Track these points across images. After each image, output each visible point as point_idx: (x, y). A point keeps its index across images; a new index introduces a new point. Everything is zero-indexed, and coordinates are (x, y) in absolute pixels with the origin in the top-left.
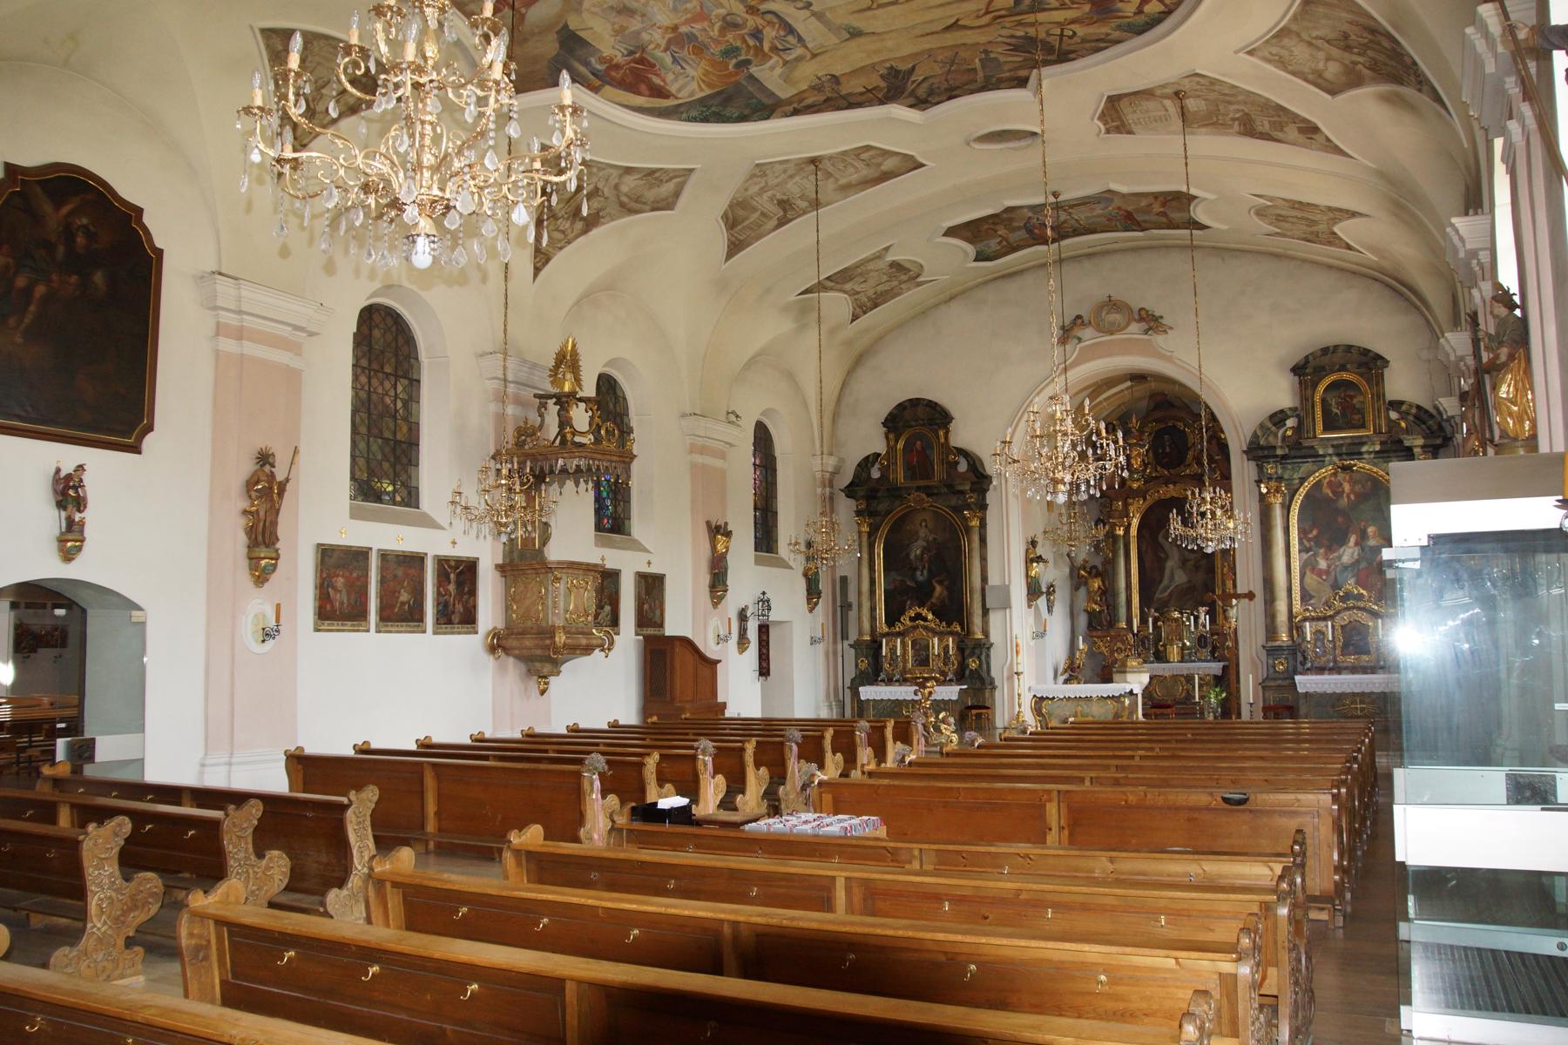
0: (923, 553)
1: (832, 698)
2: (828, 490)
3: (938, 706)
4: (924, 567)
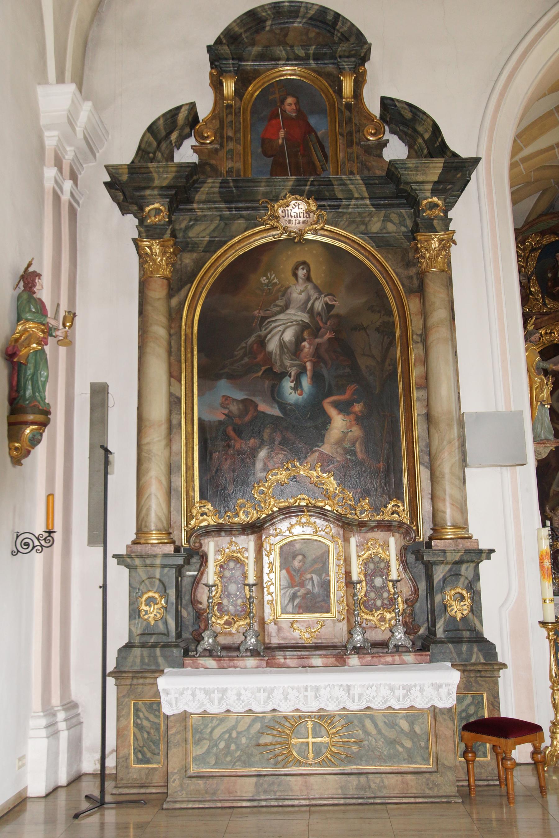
0: (299, 339)
1: (56, 700)
2: (68, 185)
3: (392, 725)
4: (302, 371)
